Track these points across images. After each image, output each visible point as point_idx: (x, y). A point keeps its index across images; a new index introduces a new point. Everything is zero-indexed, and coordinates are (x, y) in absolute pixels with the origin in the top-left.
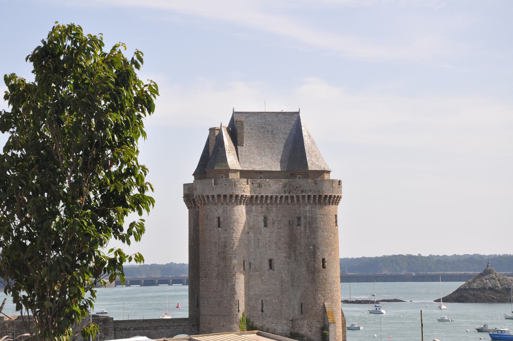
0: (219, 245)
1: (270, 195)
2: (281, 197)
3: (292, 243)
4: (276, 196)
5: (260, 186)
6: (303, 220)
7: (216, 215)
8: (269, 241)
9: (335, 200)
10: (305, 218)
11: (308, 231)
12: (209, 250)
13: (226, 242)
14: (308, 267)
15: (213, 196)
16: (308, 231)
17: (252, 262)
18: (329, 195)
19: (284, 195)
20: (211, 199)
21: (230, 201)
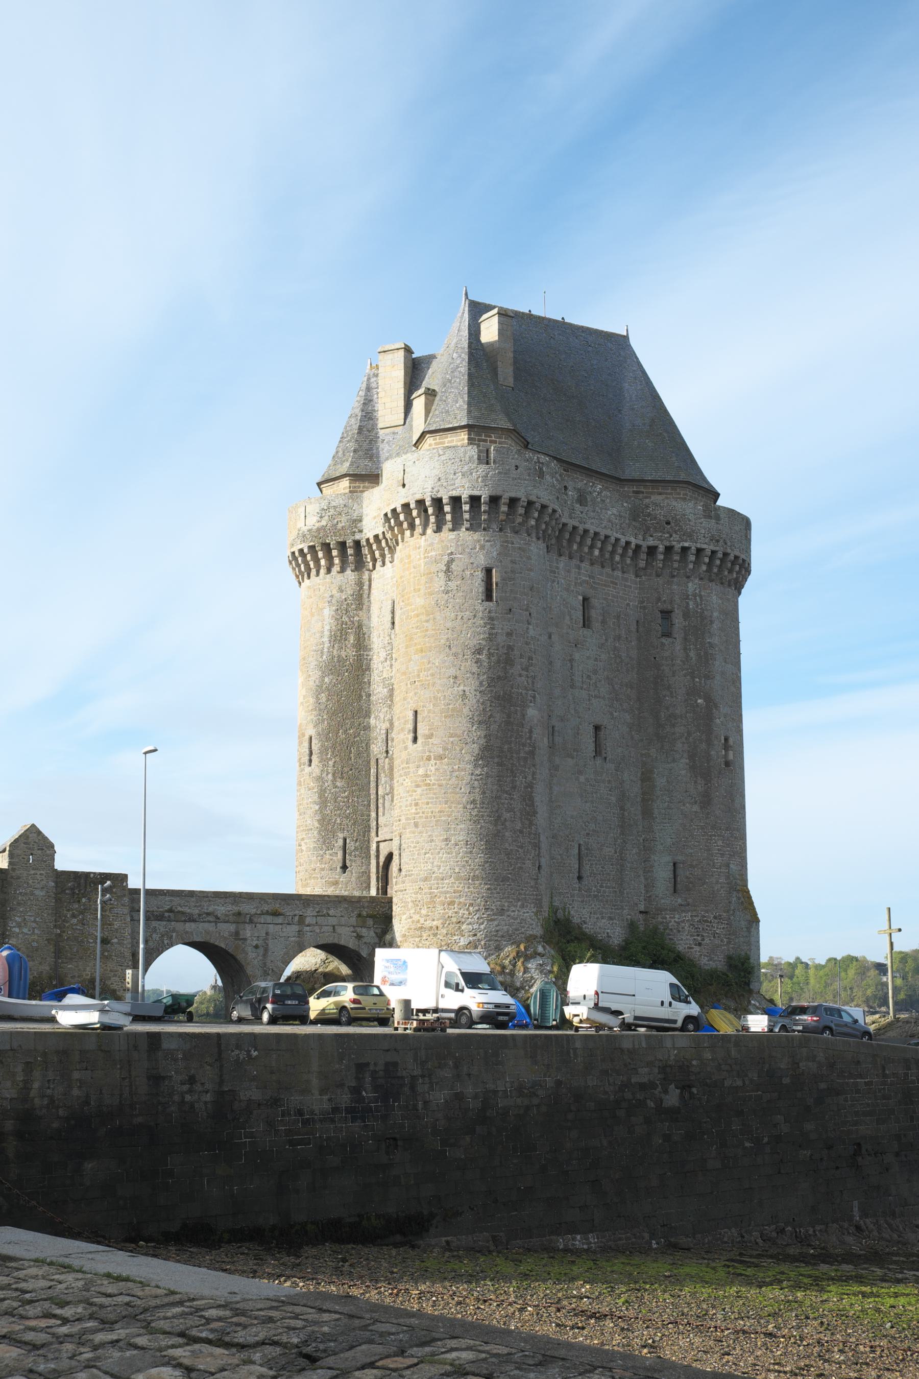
2: (628, 543)
5: (582, 499)
6: (678, 620)
10: (686, 615)
13: (510, 648)
14: (692, 757)
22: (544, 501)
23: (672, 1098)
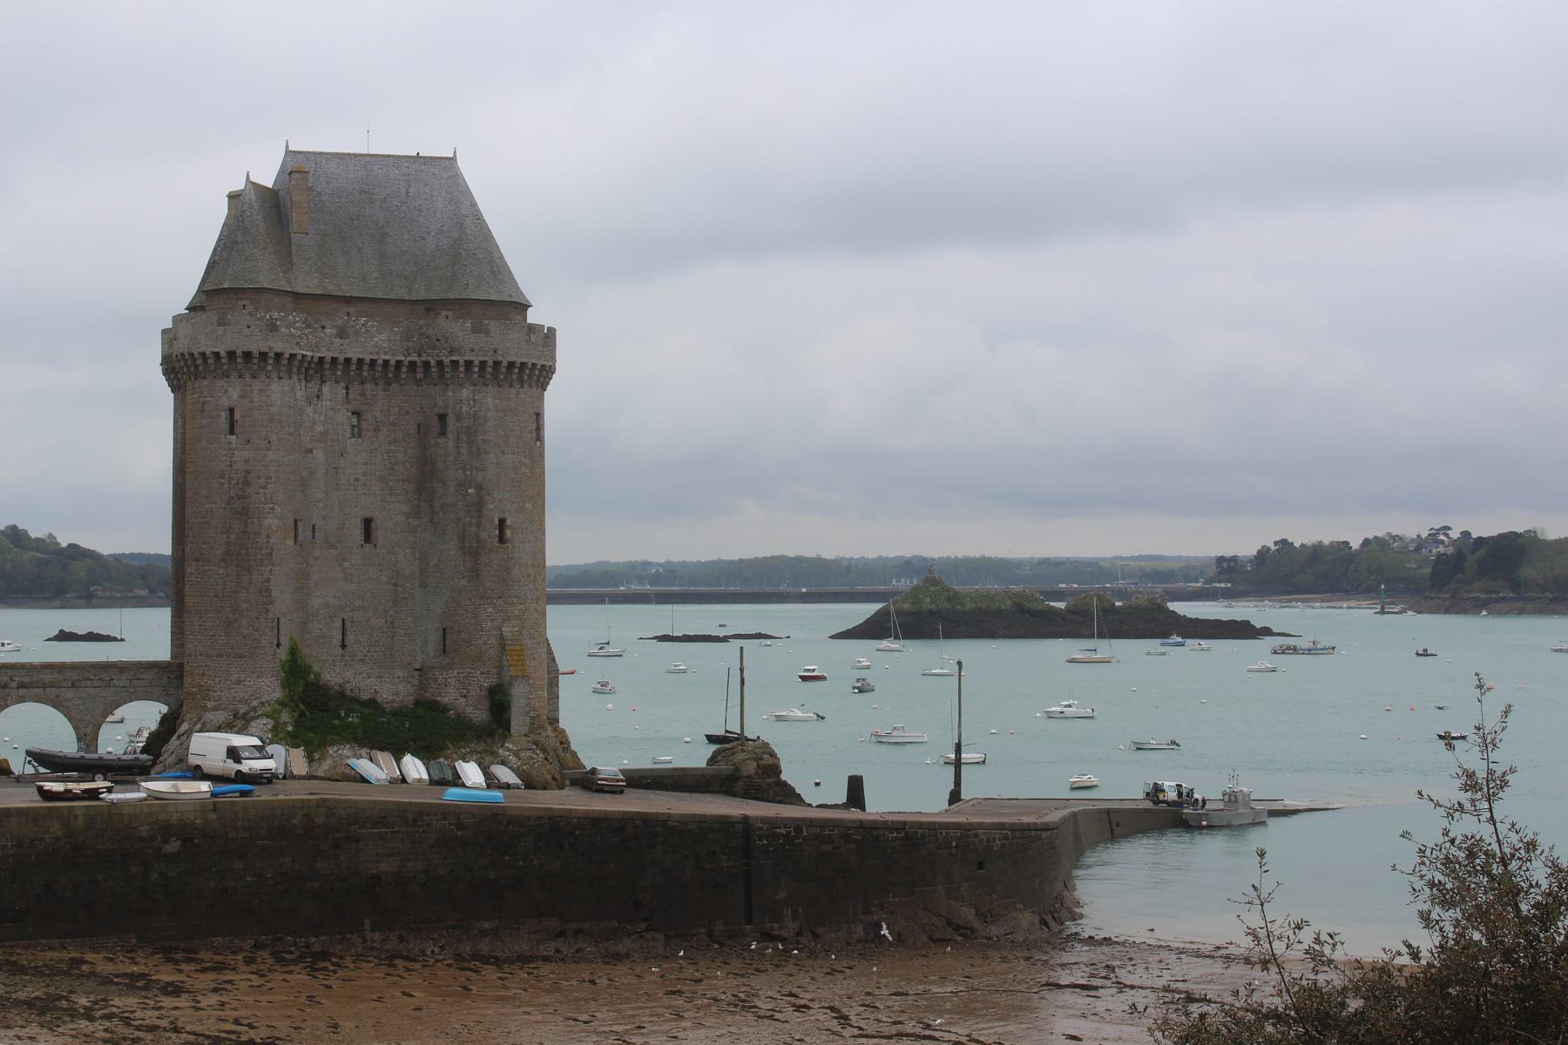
0: (230, 479)
1: (367, 358)
3: (424, 479)
4: (386, 362)
5: (342, 333)
6: (452, 423)
7: (225, 402)
8: (365, 474)
9: (541, 374)
11: (464, 451)
12: (204, 492)
14: (462, 538)
15: (217, 354)
16: (464, 451)
17: (319, 523)
18: (519, 361)
19: (406, 360)
20: (211, 361)
21: (262, 368)
22: (277, 350)
23: (173, 846)
